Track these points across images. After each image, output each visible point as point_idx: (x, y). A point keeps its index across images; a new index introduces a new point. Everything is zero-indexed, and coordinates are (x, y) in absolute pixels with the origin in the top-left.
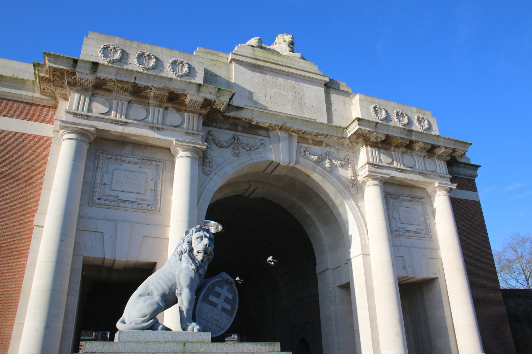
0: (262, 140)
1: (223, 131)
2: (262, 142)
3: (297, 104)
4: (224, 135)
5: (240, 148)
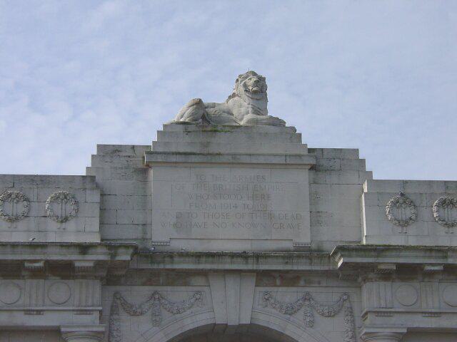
0: (198, 292)
1: (136, 288)
4: (138, 294)
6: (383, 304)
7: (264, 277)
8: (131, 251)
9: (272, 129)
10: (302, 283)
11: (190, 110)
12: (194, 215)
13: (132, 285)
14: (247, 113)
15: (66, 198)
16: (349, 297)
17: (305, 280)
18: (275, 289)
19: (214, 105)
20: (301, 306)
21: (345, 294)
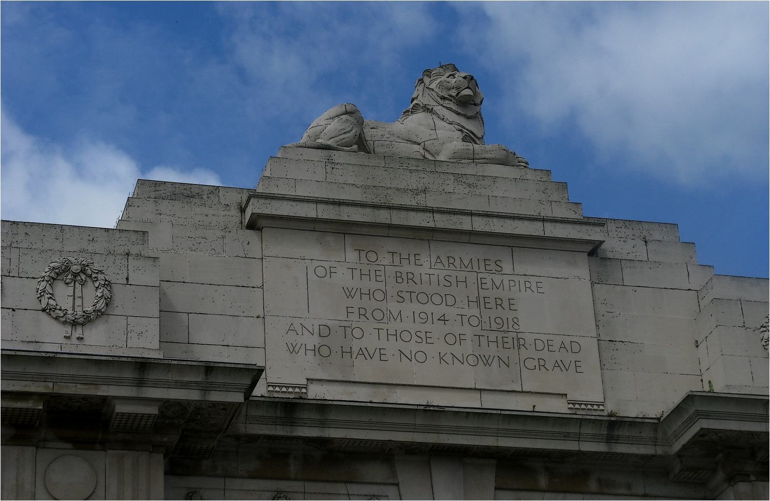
1: (237, 483)
10: (593, 485)
12: (357, 333)
13: (226, 476)
15: (83, 271)
17: (599, 481)
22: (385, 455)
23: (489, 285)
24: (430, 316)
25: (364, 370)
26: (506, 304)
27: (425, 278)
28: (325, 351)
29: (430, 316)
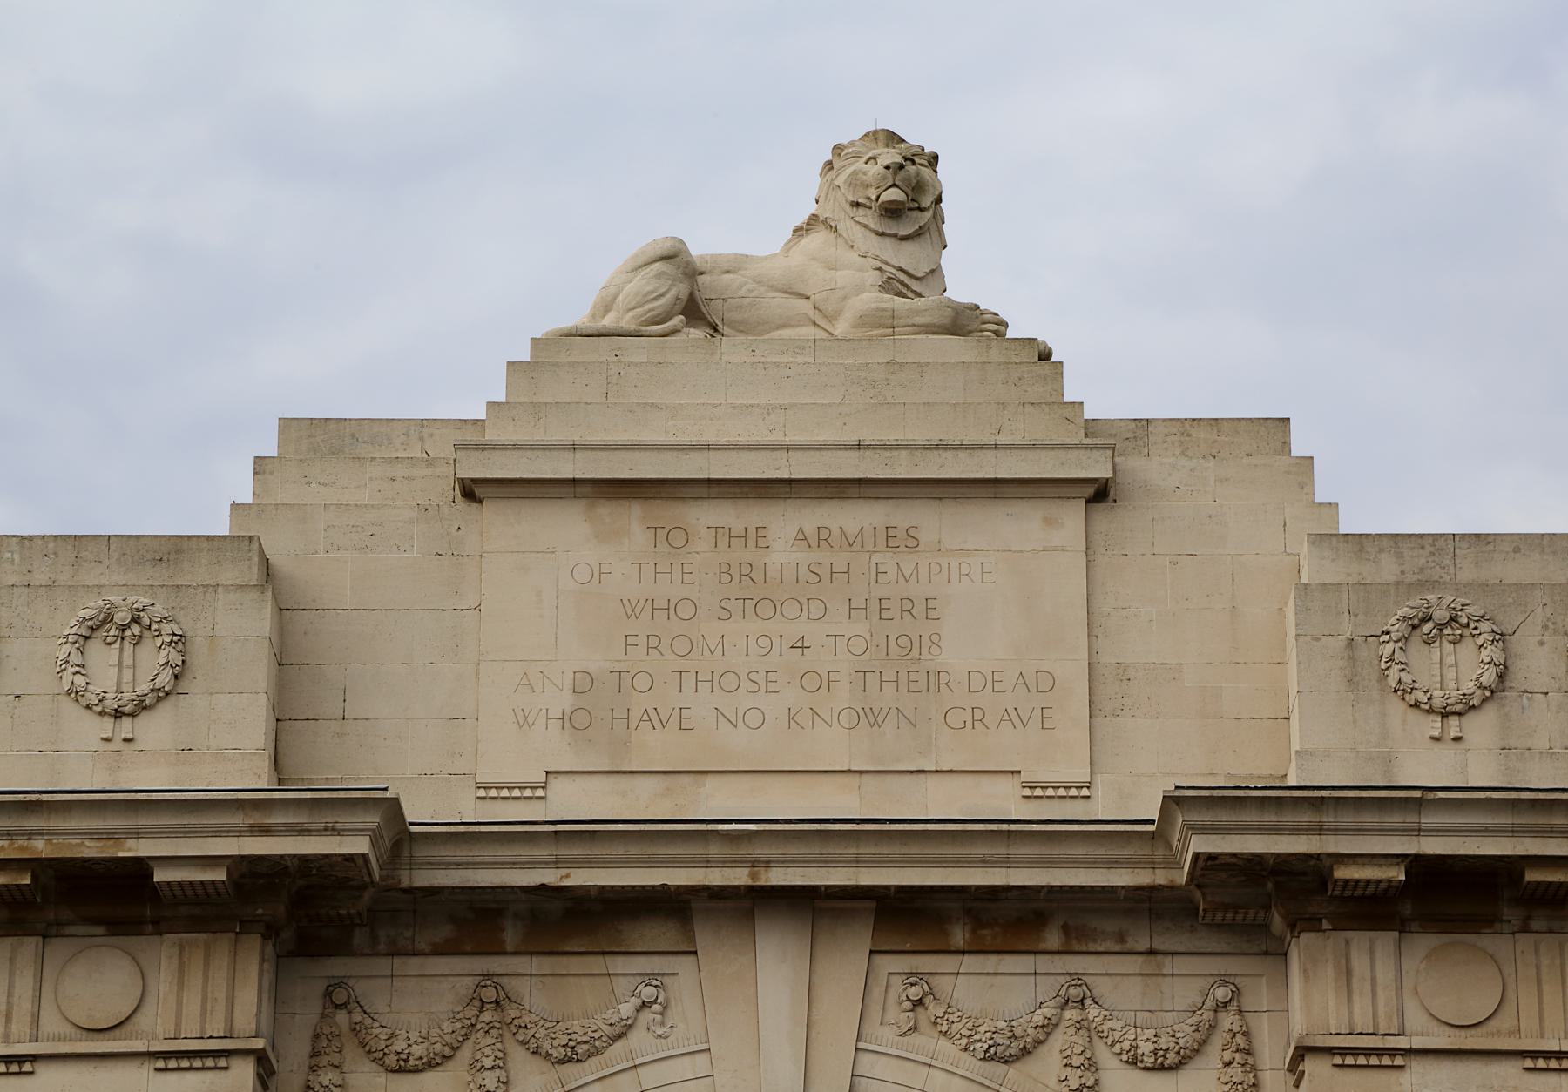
1: (414, 965)
2: (648, 992)
3: (889, 689)
5: (518, 1056)
6: (1363, 1021)
7: (909, 919)
8: (373, 819)
9: (953, 348)
10: (1053, 939)
11: (642, 283)
12: (642, 682)
13: (394, 953)
14: (859, 289)
15: (136, 620)
16: (1237, 992)
17: (1066, 929)
18: (947, 963)
19: (735, 265)
20: (1049, 1027)
21: (1223, 981)
22: (674, 907)
23: (892, 575)
24: (776, 641)
25: (654, 748)
26: (919, 609)
27: (773, 571)
28: (581, 719)
29: (776, 641)
